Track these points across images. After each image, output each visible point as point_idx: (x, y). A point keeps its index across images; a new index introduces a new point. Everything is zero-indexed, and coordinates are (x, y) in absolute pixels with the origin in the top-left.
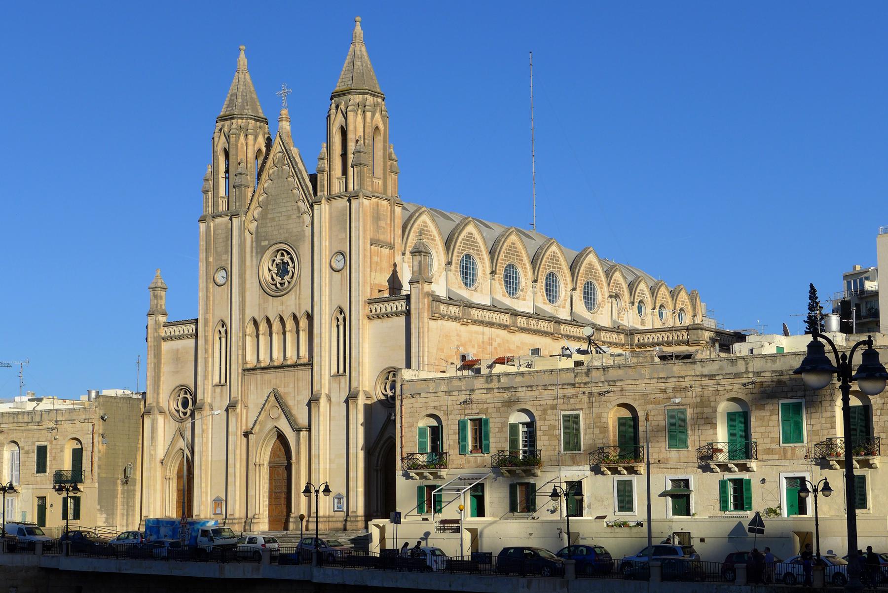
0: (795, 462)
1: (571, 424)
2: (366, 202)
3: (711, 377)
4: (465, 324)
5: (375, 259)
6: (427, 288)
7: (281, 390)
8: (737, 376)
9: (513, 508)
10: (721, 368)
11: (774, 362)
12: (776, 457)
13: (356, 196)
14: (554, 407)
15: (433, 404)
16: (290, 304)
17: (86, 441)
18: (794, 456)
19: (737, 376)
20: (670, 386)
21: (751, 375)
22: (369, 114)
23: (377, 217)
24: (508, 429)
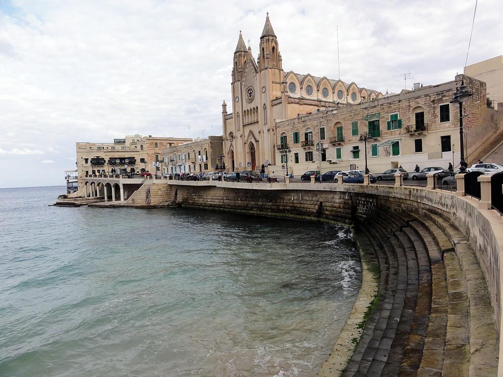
0: (396, 136)
1: (322, 130)
2: (270, 70)
3: (366, 108)
4: (302, 105)
5: (274, 87)
6: (286, 94)
7: (252, 130)
8: (375, 107)
9: (307, 160)
10: (369, 105)
11: (388, 99)
12: (389, 135)
13: (266, 69)
14: (317, 126)
15: (284, 129)
16: (253, 105)
17: (207, 148)
18: (395, 134)
19: (375, 107)
20: (352, 114)
21: (379, 106)
22: (270, 42)
23: (274, 75)
24: (304, 135)
